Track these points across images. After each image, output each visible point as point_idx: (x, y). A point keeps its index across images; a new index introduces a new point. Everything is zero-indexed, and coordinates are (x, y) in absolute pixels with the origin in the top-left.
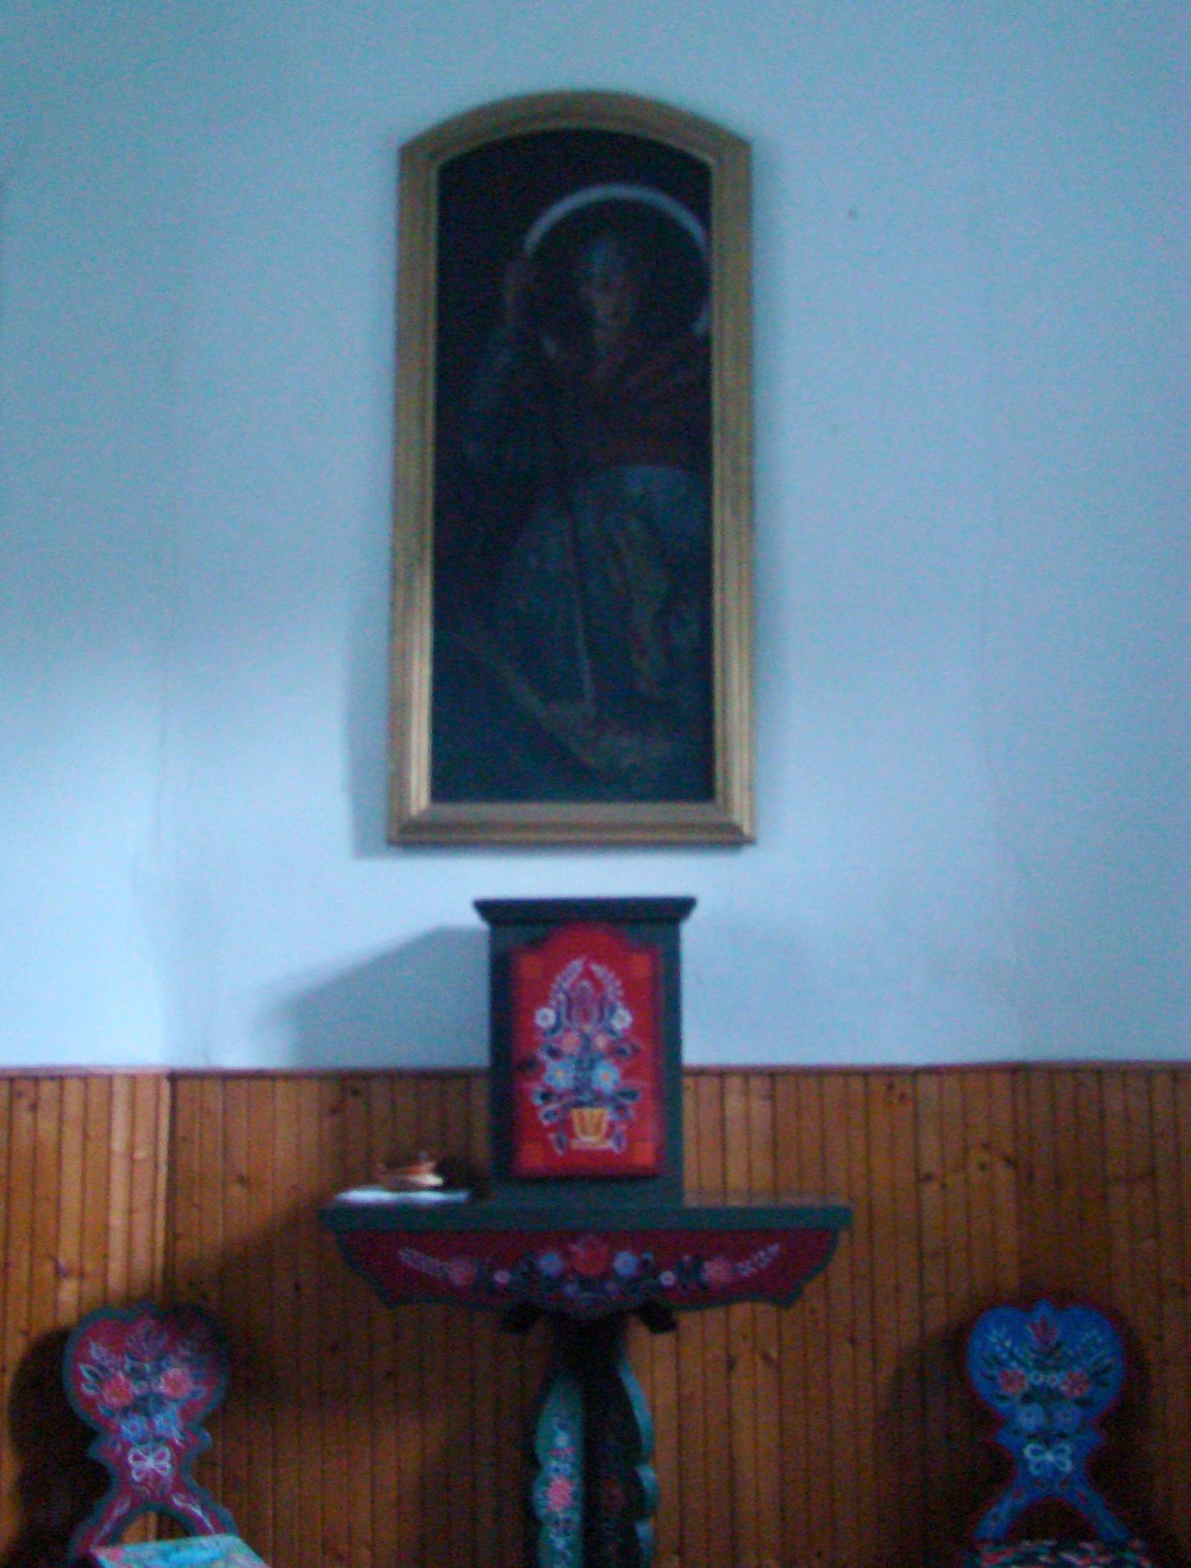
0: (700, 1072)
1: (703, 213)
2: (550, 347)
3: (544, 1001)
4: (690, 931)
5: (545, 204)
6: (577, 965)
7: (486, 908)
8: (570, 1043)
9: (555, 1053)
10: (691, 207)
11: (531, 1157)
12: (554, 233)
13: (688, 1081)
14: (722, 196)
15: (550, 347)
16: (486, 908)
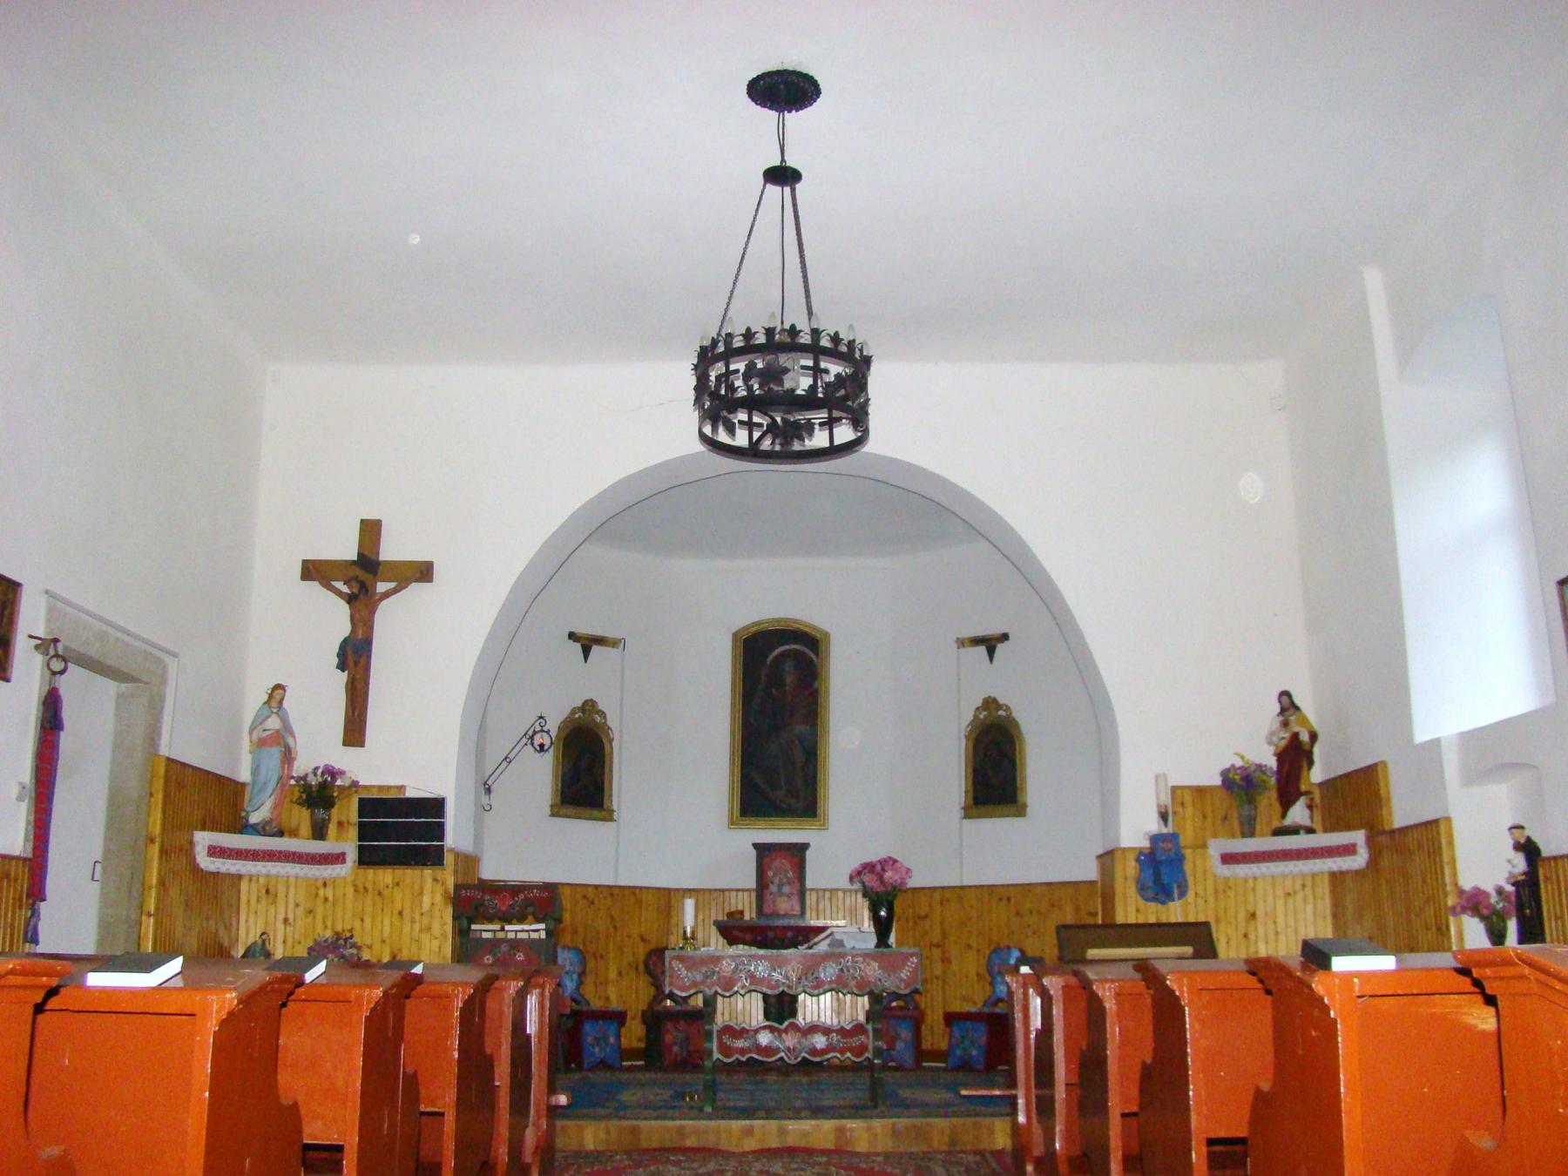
0: (812, 890)
1: (817, 655)
2: (774, 690)
3: (770, 869)
4: (809, 854)
5: (774, 649)
6: (778, 860)
7: (756, 846)
8: (777, 881)
9: (772, 883)
10: (812, 651)
11: (766, 910)
12: (776, 657)
13: (808, 893)
14: (822, 647)
15: (774, 690)
16: (756, 846)
